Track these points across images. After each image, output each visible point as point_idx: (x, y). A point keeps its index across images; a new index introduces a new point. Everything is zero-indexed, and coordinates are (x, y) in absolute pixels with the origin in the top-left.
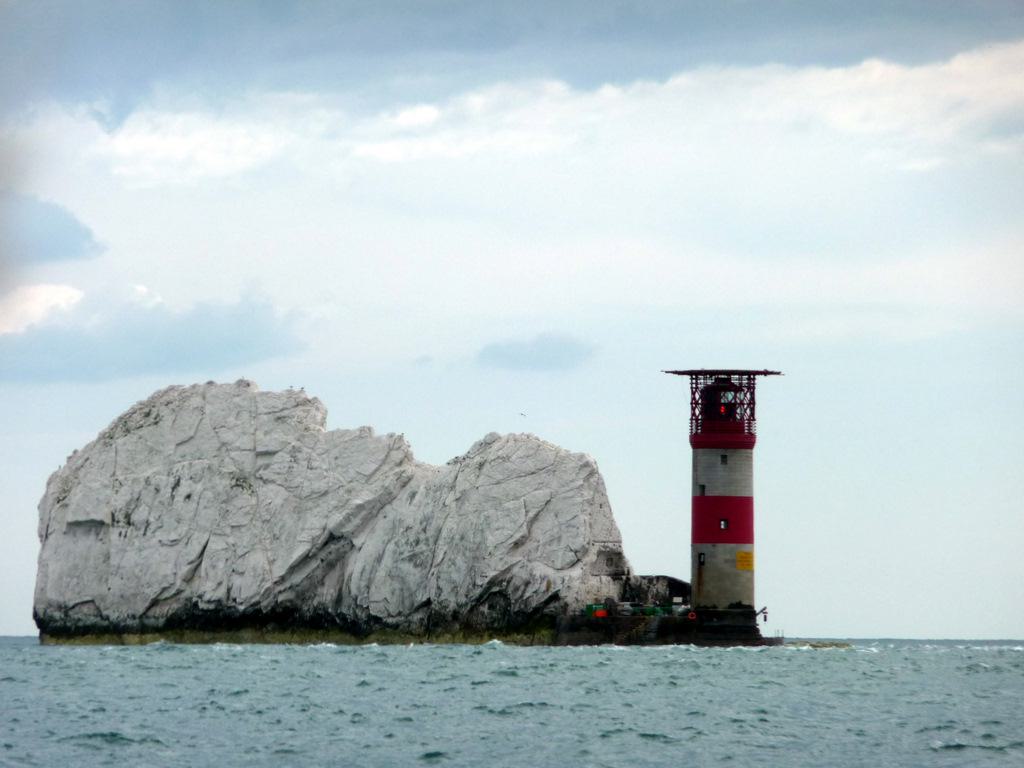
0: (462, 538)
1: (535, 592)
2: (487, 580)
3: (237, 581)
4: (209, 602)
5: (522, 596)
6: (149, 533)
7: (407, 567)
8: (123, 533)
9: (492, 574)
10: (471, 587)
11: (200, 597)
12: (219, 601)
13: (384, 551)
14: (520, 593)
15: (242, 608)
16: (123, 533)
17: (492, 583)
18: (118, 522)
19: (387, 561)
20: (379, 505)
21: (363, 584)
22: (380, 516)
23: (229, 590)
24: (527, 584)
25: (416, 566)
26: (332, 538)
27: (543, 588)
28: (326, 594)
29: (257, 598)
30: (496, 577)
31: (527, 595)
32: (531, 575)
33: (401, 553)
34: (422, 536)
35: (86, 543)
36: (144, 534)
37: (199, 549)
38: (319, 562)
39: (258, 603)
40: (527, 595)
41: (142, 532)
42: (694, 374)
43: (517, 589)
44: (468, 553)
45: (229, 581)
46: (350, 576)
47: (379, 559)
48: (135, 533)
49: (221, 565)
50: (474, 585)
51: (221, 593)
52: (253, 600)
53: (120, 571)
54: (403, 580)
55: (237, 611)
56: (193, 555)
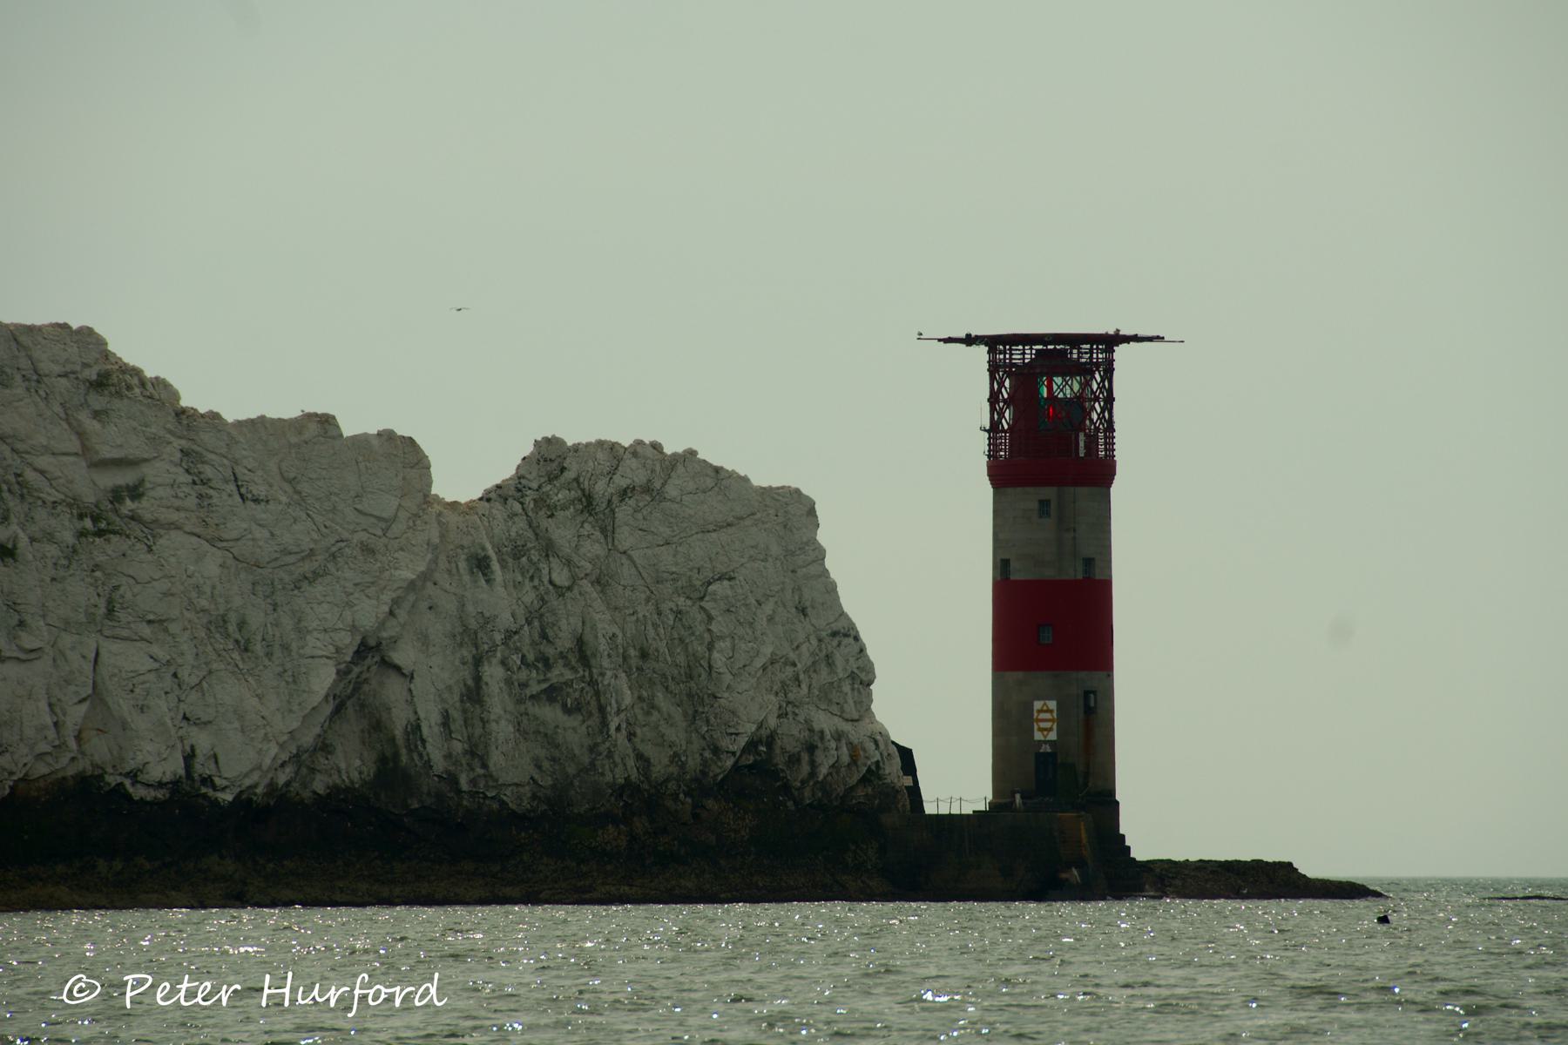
0: (644, 655)
2: (742, 741)
5: (813, 774)
7: (550, 714)
10: (707, 754)
12: (176, 783)
13: (478, 679)
14: (805, 769)
15: (228, 797)
17: (752, 745)
19: (498, 701)
21: (458, 747)
23: (189, 758)
24: (811, 749)
25: (568, 711)
28: (351, 764)
31: (823, 771)
32: (811, 730)
33: (523, 685)
34: (550, 651)
42: (993, 343)
43: (794, 760)
44: (672, 687)
46: (415, 728)
47: (474, 694)
50: (716, 750)
51: (173, 767)
54: (550, 740)
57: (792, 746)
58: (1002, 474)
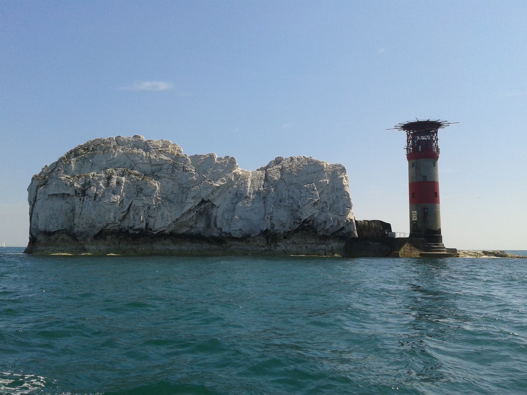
1: (331, 226)
3: (151, 221)
4: (136, 230)
6: (97, 199)
8: (82, 199)
9: (304, 217)
11: (131, 228)
15: (156, 233)
16: (82, 199)
18: (79, 194)
20: (227, 187)
22: (227, 192)
23: (147, 225)
24: (325, 222)
26: (203, 201)
27: (336, 224)
29: (164, 229)
30: (305, 220)
35: (59, 203)
36: (95, 199)
37: (127, 207)
38: (195, 212)
39: (164, 231)
40: (327, 227)
41: (93, 198)
45: (147, 220)
48: (89, 199)
49: (142, 213)
51: (143, 226)
52: (162, 230)
53: (82, 216)
55: (153, 234)
56: (125, 209)
57: (319, 221)
58: (410, 157)
